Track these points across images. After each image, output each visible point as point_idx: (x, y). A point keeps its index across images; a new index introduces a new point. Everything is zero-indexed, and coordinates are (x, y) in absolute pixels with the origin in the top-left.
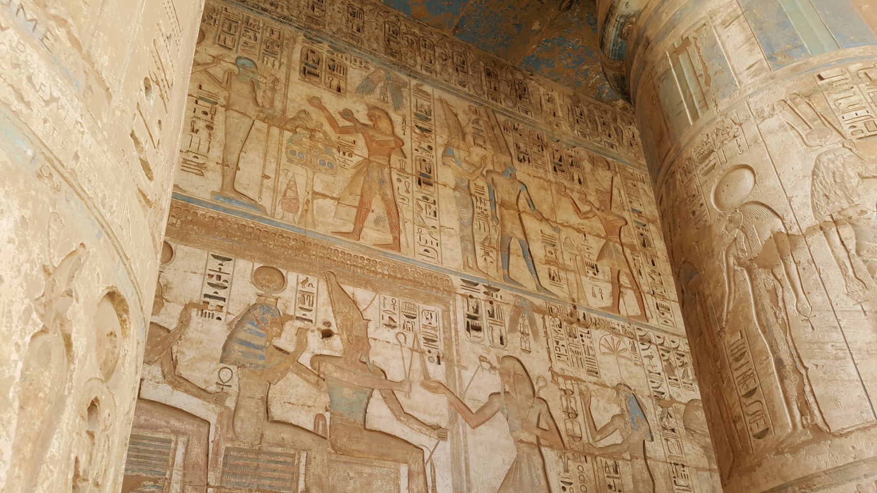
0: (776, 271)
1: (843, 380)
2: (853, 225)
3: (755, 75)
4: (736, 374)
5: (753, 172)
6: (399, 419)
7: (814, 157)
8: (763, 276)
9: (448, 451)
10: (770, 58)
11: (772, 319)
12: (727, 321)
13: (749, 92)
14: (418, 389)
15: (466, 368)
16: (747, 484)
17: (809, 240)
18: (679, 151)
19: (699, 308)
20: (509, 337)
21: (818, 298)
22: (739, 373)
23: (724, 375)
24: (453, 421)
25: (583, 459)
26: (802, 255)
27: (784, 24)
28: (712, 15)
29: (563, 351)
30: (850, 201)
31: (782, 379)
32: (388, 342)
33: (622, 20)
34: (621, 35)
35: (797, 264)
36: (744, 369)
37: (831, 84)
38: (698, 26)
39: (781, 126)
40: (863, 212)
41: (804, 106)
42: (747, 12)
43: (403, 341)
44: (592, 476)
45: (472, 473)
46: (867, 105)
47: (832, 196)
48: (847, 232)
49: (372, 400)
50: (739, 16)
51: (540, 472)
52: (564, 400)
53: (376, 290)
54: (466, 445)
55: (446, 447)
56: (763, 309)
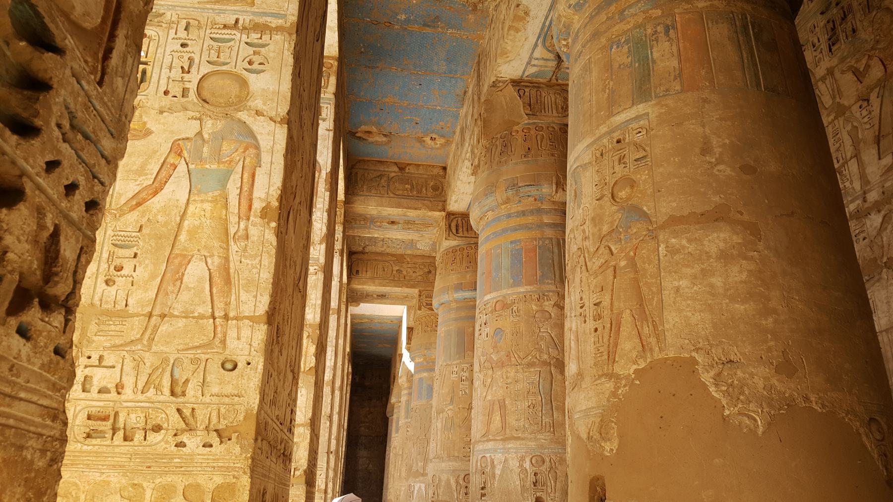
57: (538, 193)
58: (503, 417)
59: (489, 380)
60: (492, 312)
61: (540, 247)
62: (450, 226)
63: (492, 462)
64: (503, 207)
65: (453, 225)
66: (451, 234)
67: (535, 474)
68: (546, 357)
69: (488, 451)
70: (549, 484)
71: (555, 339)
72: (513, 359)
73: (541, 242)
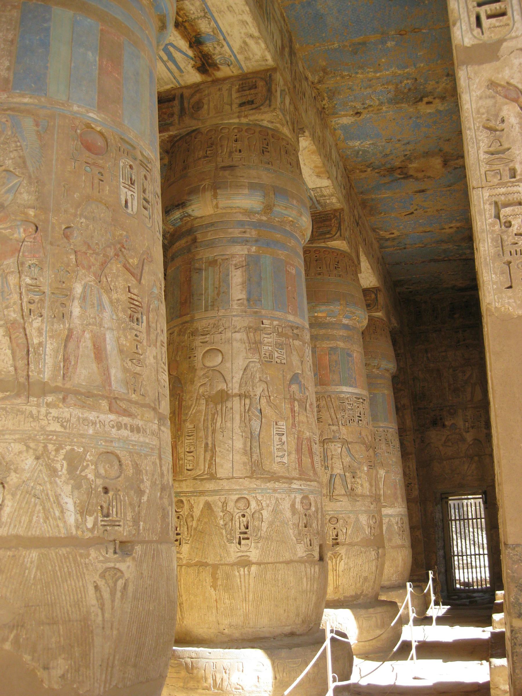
0: (218, 406)
1: (227, 459)
2: (250, 399)
3: (239, 306)
4: (186, 441)
5: (223, 355)
7: (248, 362)
8: (211, 405)
10: (248, 300)
11: (210, 426)
12: (190, 417)
13: (234, 314)
16: (177, 486)
17: (234, 399)
18: (192, 320)
19: (177, 403)
21: (229, 424)
22: (188, 441)
23: (181, 439)
26: (229, 404)
27: (259, 284)
28: (233, 256)
30: (253, 389)
31: (206, 451)
33: (186, 214)
34: (181, 219)
35: (226, 407)
36: (191, 441)
37: (265, 328)
38: (224, 257)
39: (241, 340)
40: (255, 395)
41: (252, 334)
42: (247, 266)
46: (272, 345)
47: (248, 383)
48: (248, 401)
50: (243, 267)
56: (208, 419)
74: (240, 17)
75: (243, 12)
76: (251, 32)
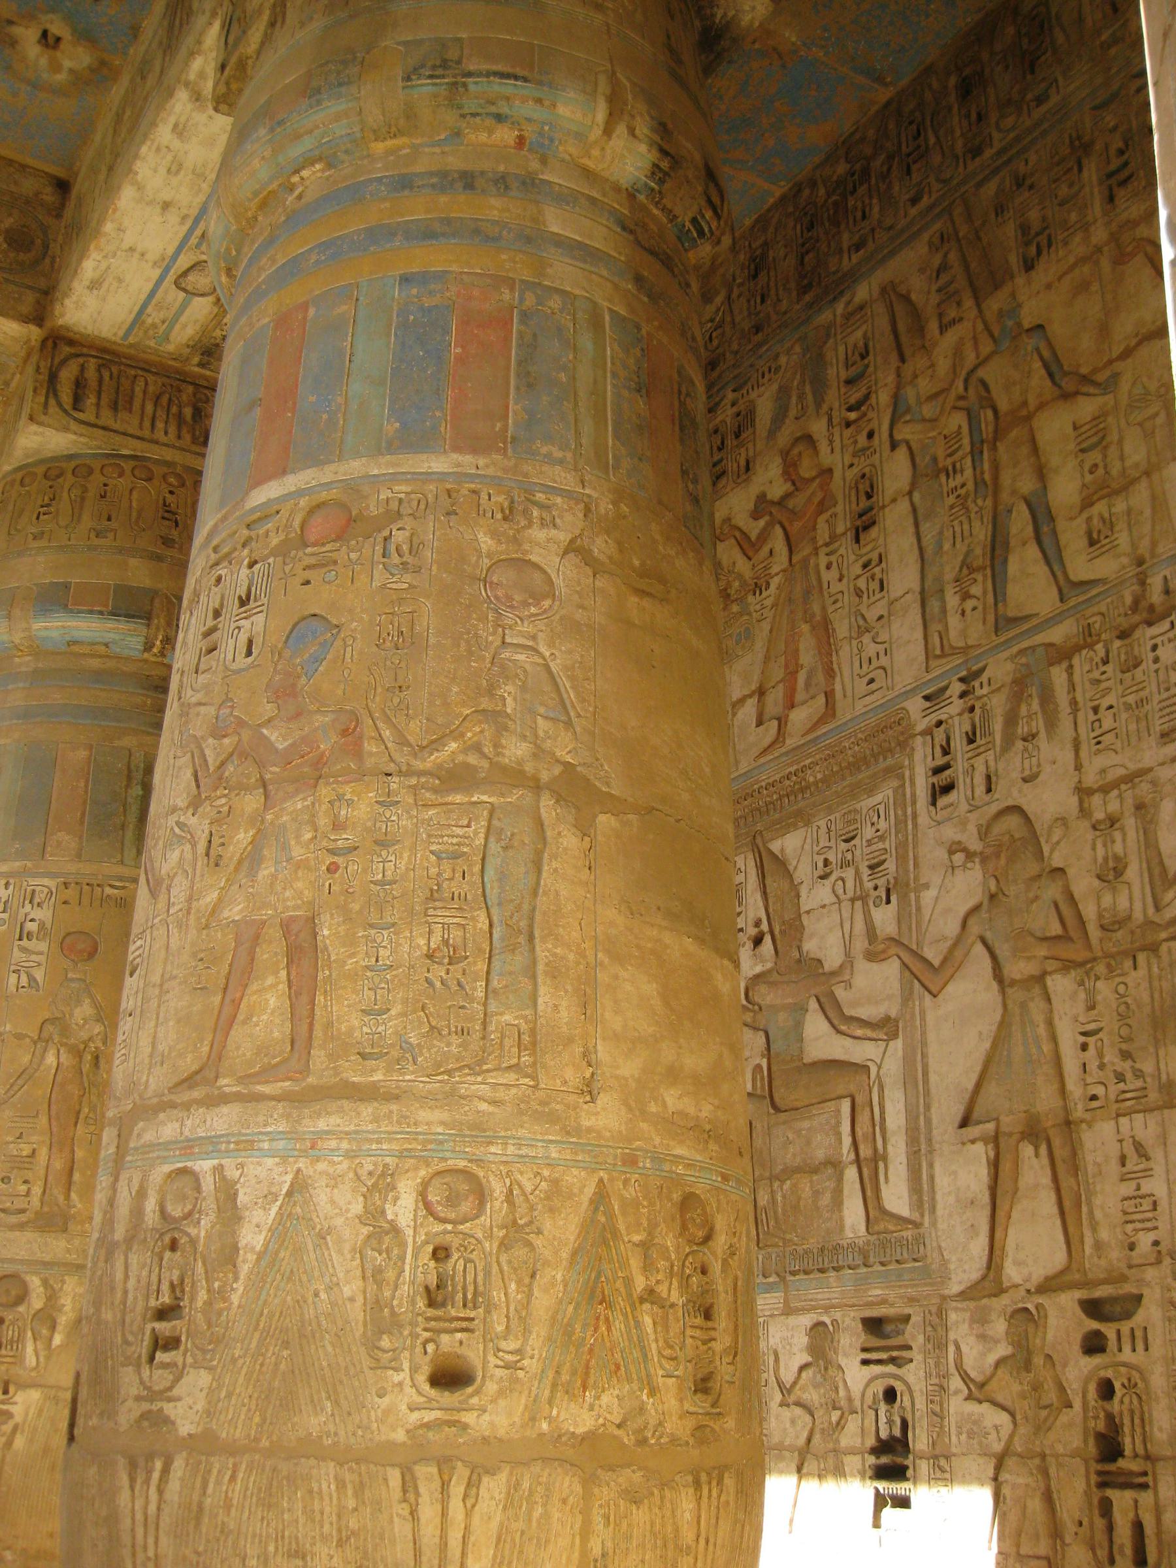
6: (838, 1032)
9: (900, 1053)
14: (861, 965)
15: (927, 886)
20: (1001, 766)
24: (907, 998)
25: (1128, 963)
29: (1108, 723)
32: (823, 907)
43: (840, 891)
44: (1146, 998)
45: (933, 1078)
49: (808, 1017)
51: (1042, 1030)
52: (1099, 846)
53: (808, 823)
54: (923, 1033)
55: (898, 1045)
57: (538, 113)
58: (303, 993)
59: (243, 837)
60: (282, 551)
61: (525, 316)
62: (53, 378)
63: (228, 1193)
64: (379, 147)
65: (67, 375)
66: (53, 408)
67: (440, 1253)
68: (516, 750)
69: (212, 1144)
70: (497, 1295)
71: (565, 683)
72: (370, 747)
73: (530, 300)
74: (176, 144)
75: (158, 149)
76: (189, 106)
